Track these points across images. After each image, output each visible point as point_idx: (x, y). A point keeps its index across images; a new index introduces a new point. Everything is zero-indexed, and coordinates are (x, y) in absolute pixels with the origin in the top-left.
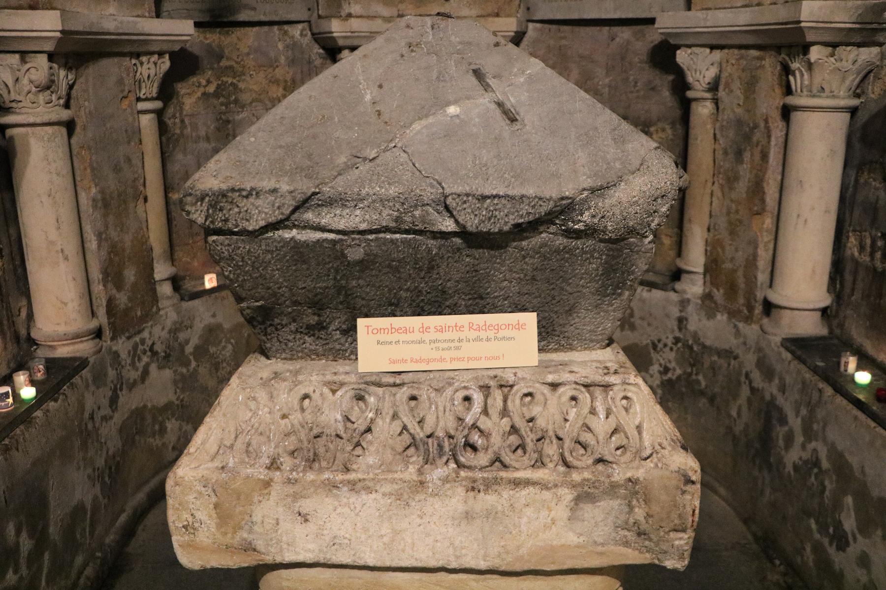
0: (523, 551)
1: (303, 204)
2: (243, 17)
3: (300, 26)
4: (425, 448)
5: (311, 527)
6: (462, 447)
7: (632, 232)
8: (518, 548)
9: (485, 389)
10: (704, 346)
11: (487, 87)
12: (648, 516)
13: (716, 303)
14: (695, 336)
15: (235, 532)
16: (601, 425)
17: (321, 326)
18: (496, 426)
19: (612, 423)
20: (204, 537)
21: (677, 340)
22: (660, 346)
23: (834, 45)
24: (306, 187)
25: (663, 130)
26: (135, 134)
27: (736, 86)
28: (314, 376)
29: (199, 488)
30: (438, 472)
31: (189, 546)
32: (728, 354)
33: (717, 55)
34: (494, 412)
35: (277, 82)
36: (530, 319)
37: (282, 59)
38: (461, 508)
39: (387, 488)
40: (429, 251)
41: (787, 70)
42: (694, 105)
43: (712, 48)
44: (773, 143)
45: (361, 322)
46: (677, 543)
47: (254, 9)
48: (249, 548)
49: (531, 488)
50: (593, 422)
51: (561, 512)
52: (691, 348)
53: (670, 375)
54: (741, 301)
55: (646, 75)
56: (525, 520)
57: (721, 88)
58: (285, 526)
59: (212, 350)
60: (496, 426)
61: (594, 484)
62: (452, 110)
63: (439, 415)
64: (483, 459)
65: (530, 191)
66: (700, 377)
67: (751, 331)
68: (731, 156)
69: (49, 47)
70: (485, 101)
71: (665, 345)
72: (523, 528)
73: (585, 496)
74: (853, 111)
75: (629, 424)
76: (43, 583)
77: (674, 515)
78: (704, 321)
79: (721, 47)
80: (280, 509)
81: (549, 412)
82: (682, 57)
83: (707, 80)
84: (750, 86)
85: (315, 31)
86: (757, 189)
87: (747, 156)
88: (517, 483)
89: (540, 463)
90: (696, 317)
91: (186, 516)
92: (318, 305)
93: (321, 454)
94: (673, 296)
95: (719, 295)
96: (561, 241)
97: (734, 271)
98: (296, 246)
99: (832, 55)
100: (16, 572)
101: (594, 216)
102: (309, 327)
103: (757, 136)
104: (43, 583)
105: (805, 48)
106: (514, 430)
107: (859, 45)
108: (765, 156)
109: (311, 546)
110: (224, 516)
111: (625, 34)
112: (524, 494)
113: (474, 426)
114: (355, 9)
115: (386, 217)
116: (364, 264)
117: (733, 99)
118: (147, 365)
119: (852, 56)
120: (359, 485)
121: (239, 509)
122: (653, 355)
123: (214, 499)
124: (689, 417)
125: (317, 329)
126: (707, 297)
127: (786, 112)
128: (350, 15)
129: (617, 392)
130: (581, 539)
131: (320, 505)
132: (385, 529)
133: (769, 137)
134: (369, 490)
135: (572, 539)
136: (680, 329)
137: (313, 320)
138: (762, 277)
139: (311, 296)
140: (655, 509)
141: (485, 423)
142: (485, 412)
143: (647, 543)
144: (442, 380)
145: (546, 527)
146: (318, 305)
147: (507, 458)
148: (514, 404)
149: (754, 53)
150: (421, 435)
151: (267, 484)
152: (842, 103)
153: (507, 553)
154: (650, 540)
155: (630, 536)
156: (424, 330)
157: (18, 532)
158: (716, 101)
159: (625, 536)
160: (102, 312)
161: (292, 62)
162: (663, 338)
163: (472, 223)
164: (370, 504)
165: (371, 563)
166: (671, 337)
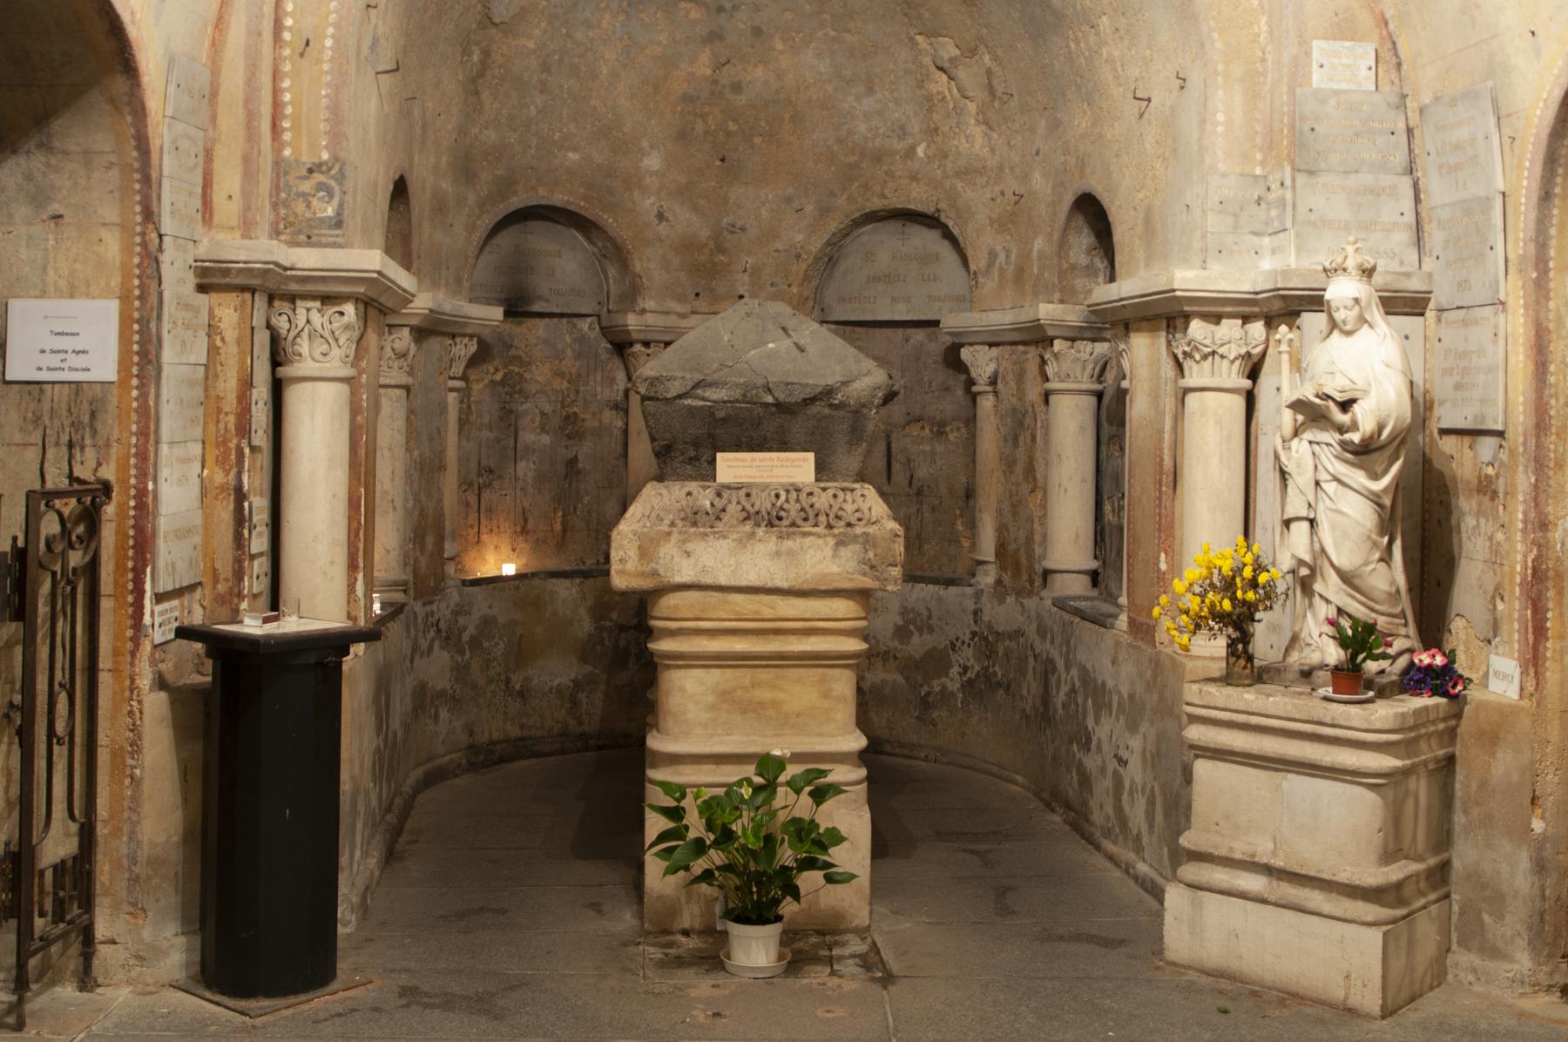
1: (697, 385)
2: (537, 307)
3: (589, 320)
5: (692, 560)
6: (774, 517)
7: (863, 406)
9: (788, 491)
10: (998, 634)
11: (789, 336)
14: (989, 625)
16: (849, 508)
17: (697, 459)
18: (793, 508)
19: (855, 506)
20: (630, 566)
21: (974, 634)
23: (1073, 340)
24: (698, 377)
26: (443, 408)
27: (1010, 377)
30: (760, 532)
31: (621, 572)
32: (1019, 633)
33: (995, 351)
34: (792, 501)
35: (561, 375)
36: (811, 456)
37: (569, 352)
39: (735, 536)
41: (1043, 362)
42: (979, 399)
43: (991, 345)
45: (719, 455)
47: (547, 301)
48: (655, 574)
50: (845, 506)
51: (828, 552)
52: (986, 639)
54: (1025, 577)
55: (942, 375)
58: (677, 559)
59: (486, 644)
60: (793, 508)
61: (844, 534)
63: (763, 503)
65: (811, 382)
66: (997, 668)
67: (1031, 603)
69: (414, 322)
70: (787, 342)
73: (840, 543)
74: (1099, 396)
75: (865, 507)
79: (997, 344)
81: (822, 501)
82: (965, 354)
84: (1020, 377)
85: (604, 324)
86: (1030, 470)
87: (1021, 439)
88: (805, 534)
89: (816, 525)
91: (621, 553)
92: (696, 444)
94: (969, 590)
95: (1007, 579)
96: (827, 411)
97: (1018, 550)
98: (690, 407)
103: (1028, 421)
105: (1051, 341)
106: (803, 509)
107: (1093, 340)
108: (1034, 438)
110: (644, 553)
111: (919, 335)
112: (809, 540)
113: (782, 508)
114: (650, 304)
115: (737, 394)
116: (724, 420)
117: (1007, 388)
118: (433, 640)
119: (1089, 349)
122: (953, 657)
125: (692, 460)
126: (999, 582)
127: (1047, 395)
128: (644, 311)
129: (858, 493)
131: (697, 546)
132: (732, 562)
134: (725, 537)
135: (835, 569)
137: (692, 453)
138: (1038, 550)
139: (690, 442)
141: (786, 506)
142: (787, 501)
144: (765, 487)
145: (821, 562)
146: (696, 444)
147: (800, 522)
148: (803, 496)
149: (1021, 348)
150: (752, 511)
151: (669, 534)
152: (1084, 387)
155: (866, 568)
156: (753, 460)
158: (996, 393)
160: (409, 569)
161: (579, 355)
163: (782, 397)
164: (725, 545)
165: (723, 581)
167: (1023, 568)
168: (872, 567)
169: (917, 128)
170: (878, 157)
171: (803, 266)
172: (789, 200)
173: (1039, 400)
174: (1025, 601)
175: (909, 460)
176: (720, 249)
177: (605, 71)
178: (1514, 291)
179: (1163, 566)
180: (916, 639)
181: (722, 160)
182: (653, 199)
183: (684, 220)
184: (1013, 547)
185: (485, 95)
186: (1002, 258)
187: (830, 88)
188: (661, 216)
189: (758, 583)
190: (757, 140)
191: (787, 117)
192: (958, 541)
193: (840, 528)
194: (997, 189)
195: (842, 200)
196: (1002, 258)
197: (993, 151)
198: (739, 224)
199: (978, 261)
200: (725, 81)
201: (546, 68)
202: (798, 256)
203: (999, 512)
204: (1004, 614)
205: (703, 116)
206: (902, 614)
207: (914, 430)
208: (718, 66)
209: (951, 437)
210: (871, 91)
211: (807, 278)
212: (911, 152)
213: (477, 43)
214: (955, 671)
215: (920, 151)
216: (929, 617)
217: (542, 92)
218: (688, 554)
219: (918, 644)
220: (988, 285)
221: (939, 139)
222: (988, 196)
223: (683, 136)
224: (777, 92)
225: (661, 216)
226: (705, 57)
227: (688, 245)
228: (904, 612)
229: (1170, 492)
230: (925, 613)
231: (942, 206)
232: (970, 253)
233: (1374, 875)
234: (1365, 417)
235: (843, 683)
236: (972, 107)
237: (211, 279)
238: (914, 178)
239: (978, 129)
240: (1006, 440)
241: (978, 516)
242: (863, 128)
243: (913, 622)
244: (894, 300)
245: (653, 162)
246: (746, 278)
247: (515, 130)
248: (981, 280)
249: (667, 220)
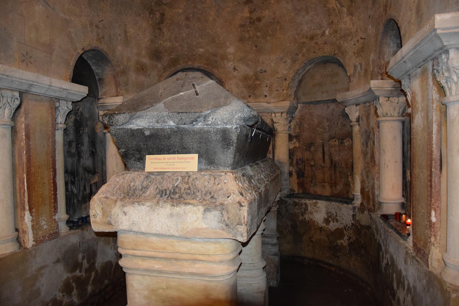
0: (189, 229)
4: (162, 193)
8: (188, 228)
9: (183, 178)
10: (361, 225)
12: (228, 218)
13: (364, 206)
14: (358, 221)
15: (106, 218)
20: (98, 219)
22: (347, 228)
25: (348, 141)
29: (98, 202)
38: (169, 212)
40: (168, 132)
44: (376, 137)
46: (240, 229)
48: (109, 223)
49: (190, 206)
51: (200, 215)
53: (351, 240)
54: (371, 203)
56: (189, 218)
57: (360, 119)
58: (120, 216)
62: (181, 94)
64: (177, 196)
68: (365, 145)
71: (349, 227)
72: (189, 221)
73: (207, 210)
76: (91, 282)
77: (237, 218)
78: (361, 215)
80: (119, 211)
83: (356, 118)
86: (373, 157)
88: (186, 204)
90: (358, 214)
97: (369, 191)
99: (388, 100)
100: (80, 272)
101: (213, 119)
102: (138, 159)
103: (371, 136)
104: (91, 282)
109: (127, 224)
111: (332, 106)
116: (150, 136)
120: (141, 203)
121: (108, 210)
123: (102, 206)
124: (359, 258)
126: (362, 204)
130: (207, 226)
131: (130, 209)
133: (374, 135)
135: (205, 226)
136: (353, 220)
137: (138, 156)
138: (377, 192)
140: (231, 215)
143: (230, 229)
152: (395, 118)
153: (184, 230)
154: (230, 228)
157: (83, 258)
159: (222, 226)
162: (348, 225)
166: (350, 223)
167: (370, 199)
168: (227, 225)
169: (325, 24)
170: (312, 38)
171: (287, 82)
172: (282, 59)
173: (375, 126)
174: (372, 214)
175: (331, 154)
176: (257, 79)
177: (211, 19)
179: (434, 219)
180: (331, 223)
181: (256, 47)
182: (231, 63)
183: (243, 69)
184: (367, 190)
185: (165, 30)
186: (359, 68)
187: (293, 15)
188: (235, 69)
189: (161, 232)
190: (268, 38)
191: (278, 28)
192: (350, 185)
193: (210, 201)
194: (356, 39)
195: (300, 56)
196: (359, 68)
197: (353, 24)
198: (264, 69)
199: (350, 71)
200: (255, 18)
201: (187, 19)
202: (286, 79)
203: (362, 175)
204: (364, 219)
205: (248, 32)
206: (327, 213)
207: (332, 142)
208: (251, 12)
209: (346, 144)
210: (308, 13)
211: (289, 87)
212: (323, 34)
213: (158, 11)
214: (346, 237)
215: (327, 33)
216: (336, 216)
217: (187, 28)
218: (125, 214)
219: (333, 226)
220: (355, 80)
221: (334, 26)
222: (353, 43)
223: (242, 40)
224: (274, 19)
225: (235, 69)
226: (246, 10)
227: (246, 78)
228: (328, 213)
229: (438, 172)
230: (335, 214)
231: (336, 52)
232: (347, 68)
236: (345, 10)
238: (325, 43)
239: (348, 18)
240: (363, 145)
241: (354, 176)
242: (305, 28)
243: (330, 217)
244: (322, 92)
245: (231, 50)
246: (267, 89)
247: (177, 42)
248: (352, 79)
249: (237, 70)
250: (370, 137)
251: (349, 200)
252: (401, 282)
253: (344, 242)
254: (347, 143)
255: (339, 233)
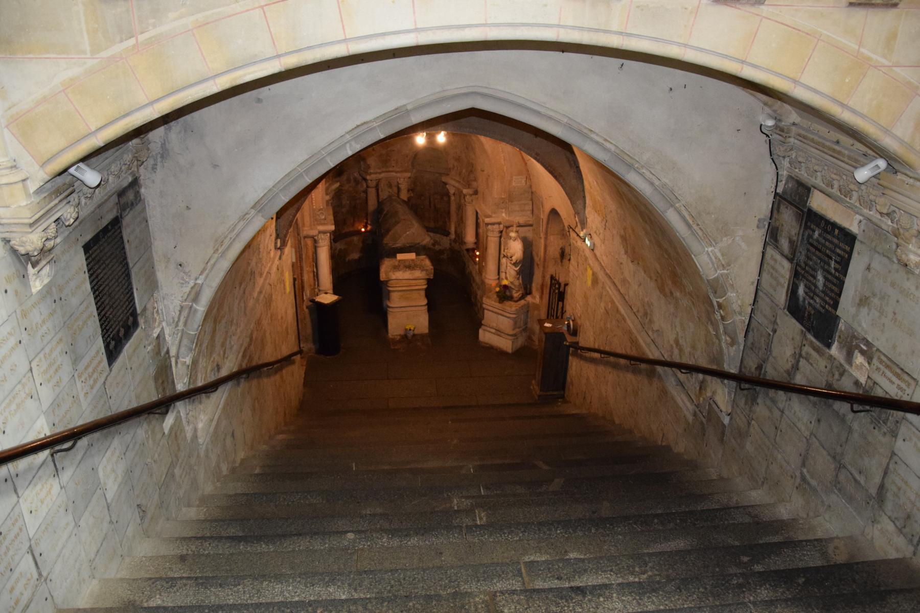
28: (394, 260)
63: (407, 264)
81: (418, 263)
86: (462, 217)
93: (396, 268)
167: (460, 238)
178: (542, 235)
193: (422, 269)
204: (456, 246)
219: (437, 248)
233: (511, 333)
234: (514, 258)
235: (423, 293)
237: (305, 237)
250: (460, 208)
251: (447, 234)
252: (474, 280)
253: (445, 256)
254: (445, 199)
255: (441, 252)
